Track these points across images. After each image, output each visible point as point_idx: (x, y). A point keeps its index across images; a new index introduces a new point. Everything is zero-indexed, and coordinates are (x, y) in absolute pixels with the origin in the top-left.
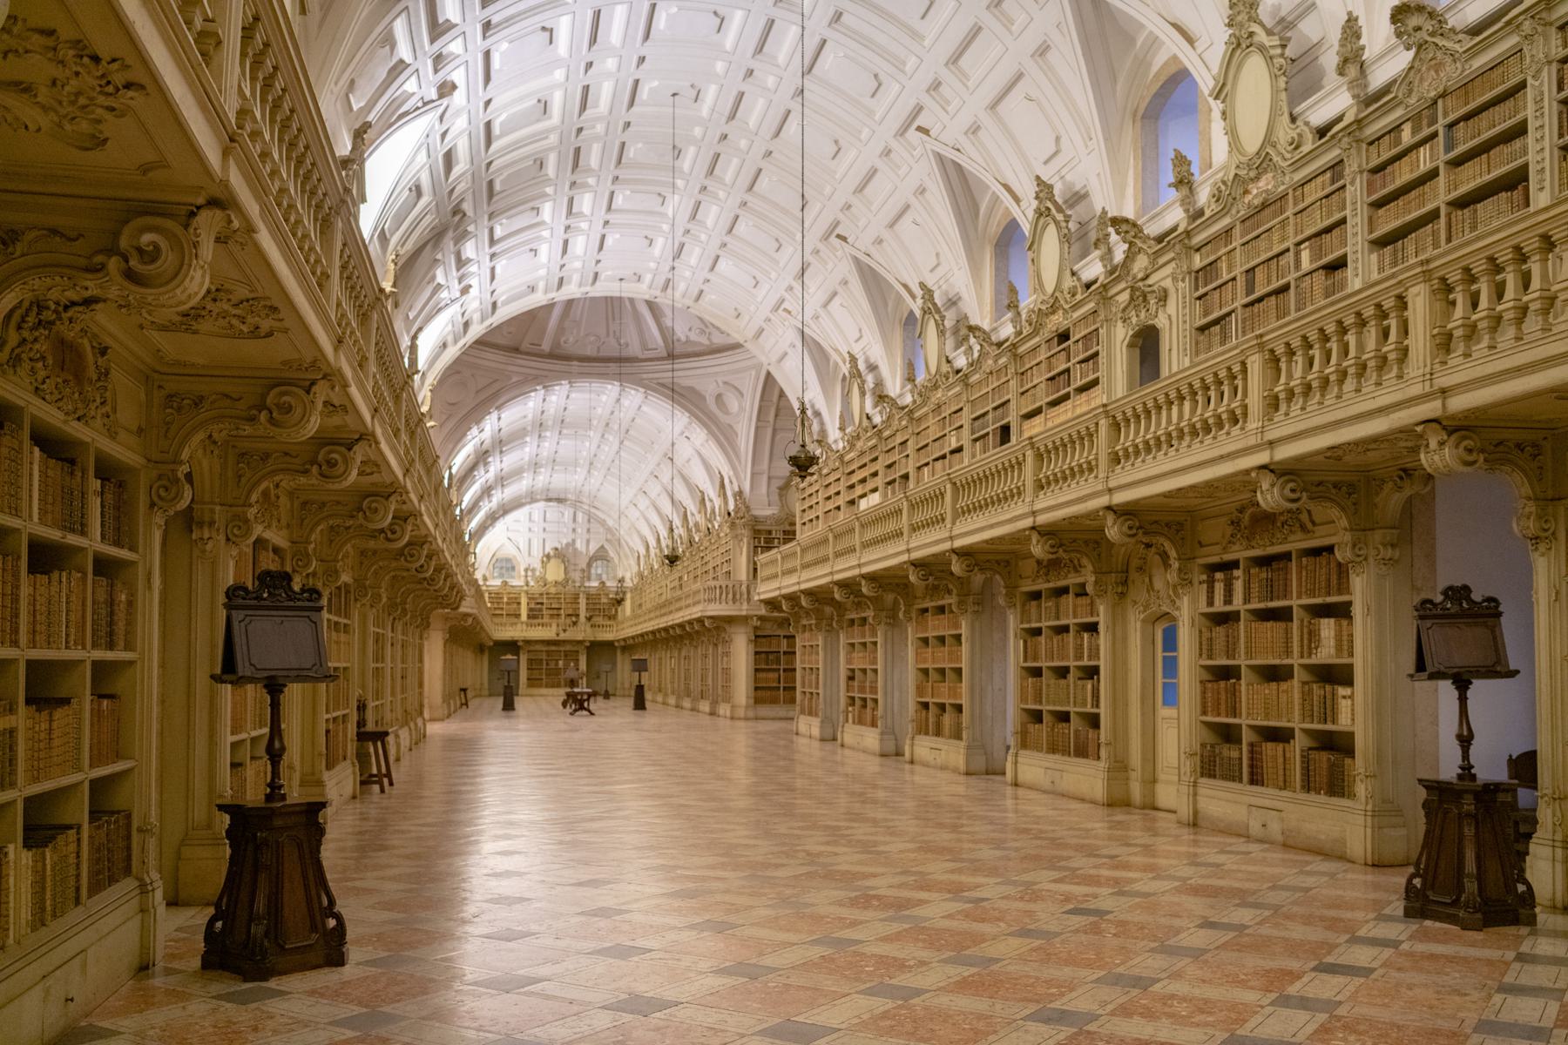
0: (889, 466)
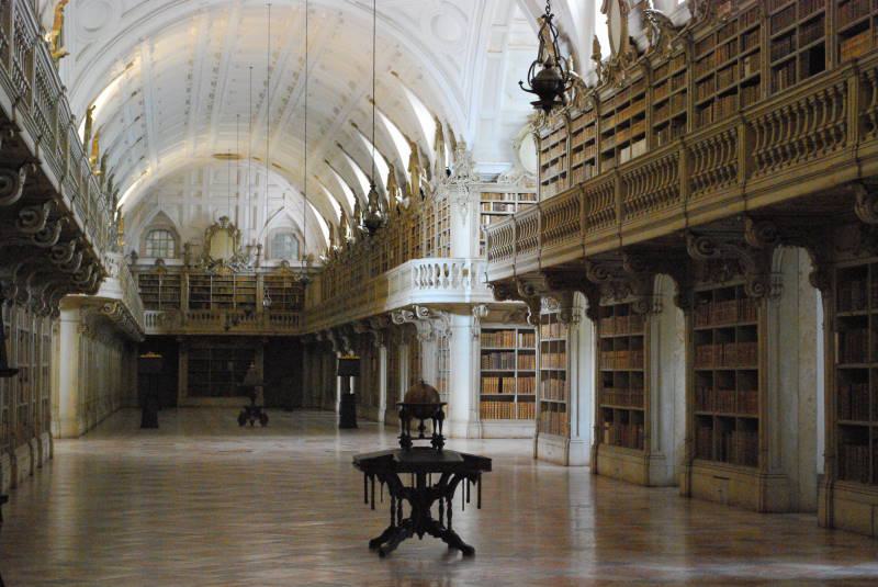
0: (659, 106)
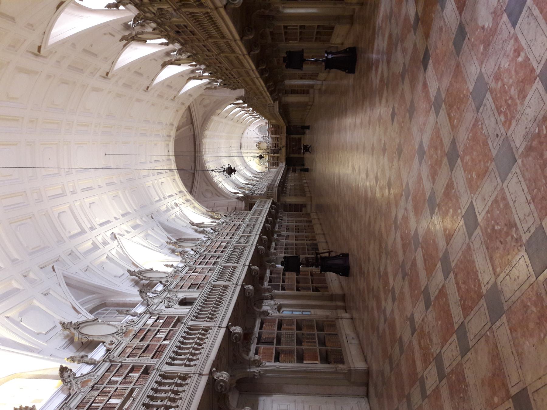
0: (227, 69)
